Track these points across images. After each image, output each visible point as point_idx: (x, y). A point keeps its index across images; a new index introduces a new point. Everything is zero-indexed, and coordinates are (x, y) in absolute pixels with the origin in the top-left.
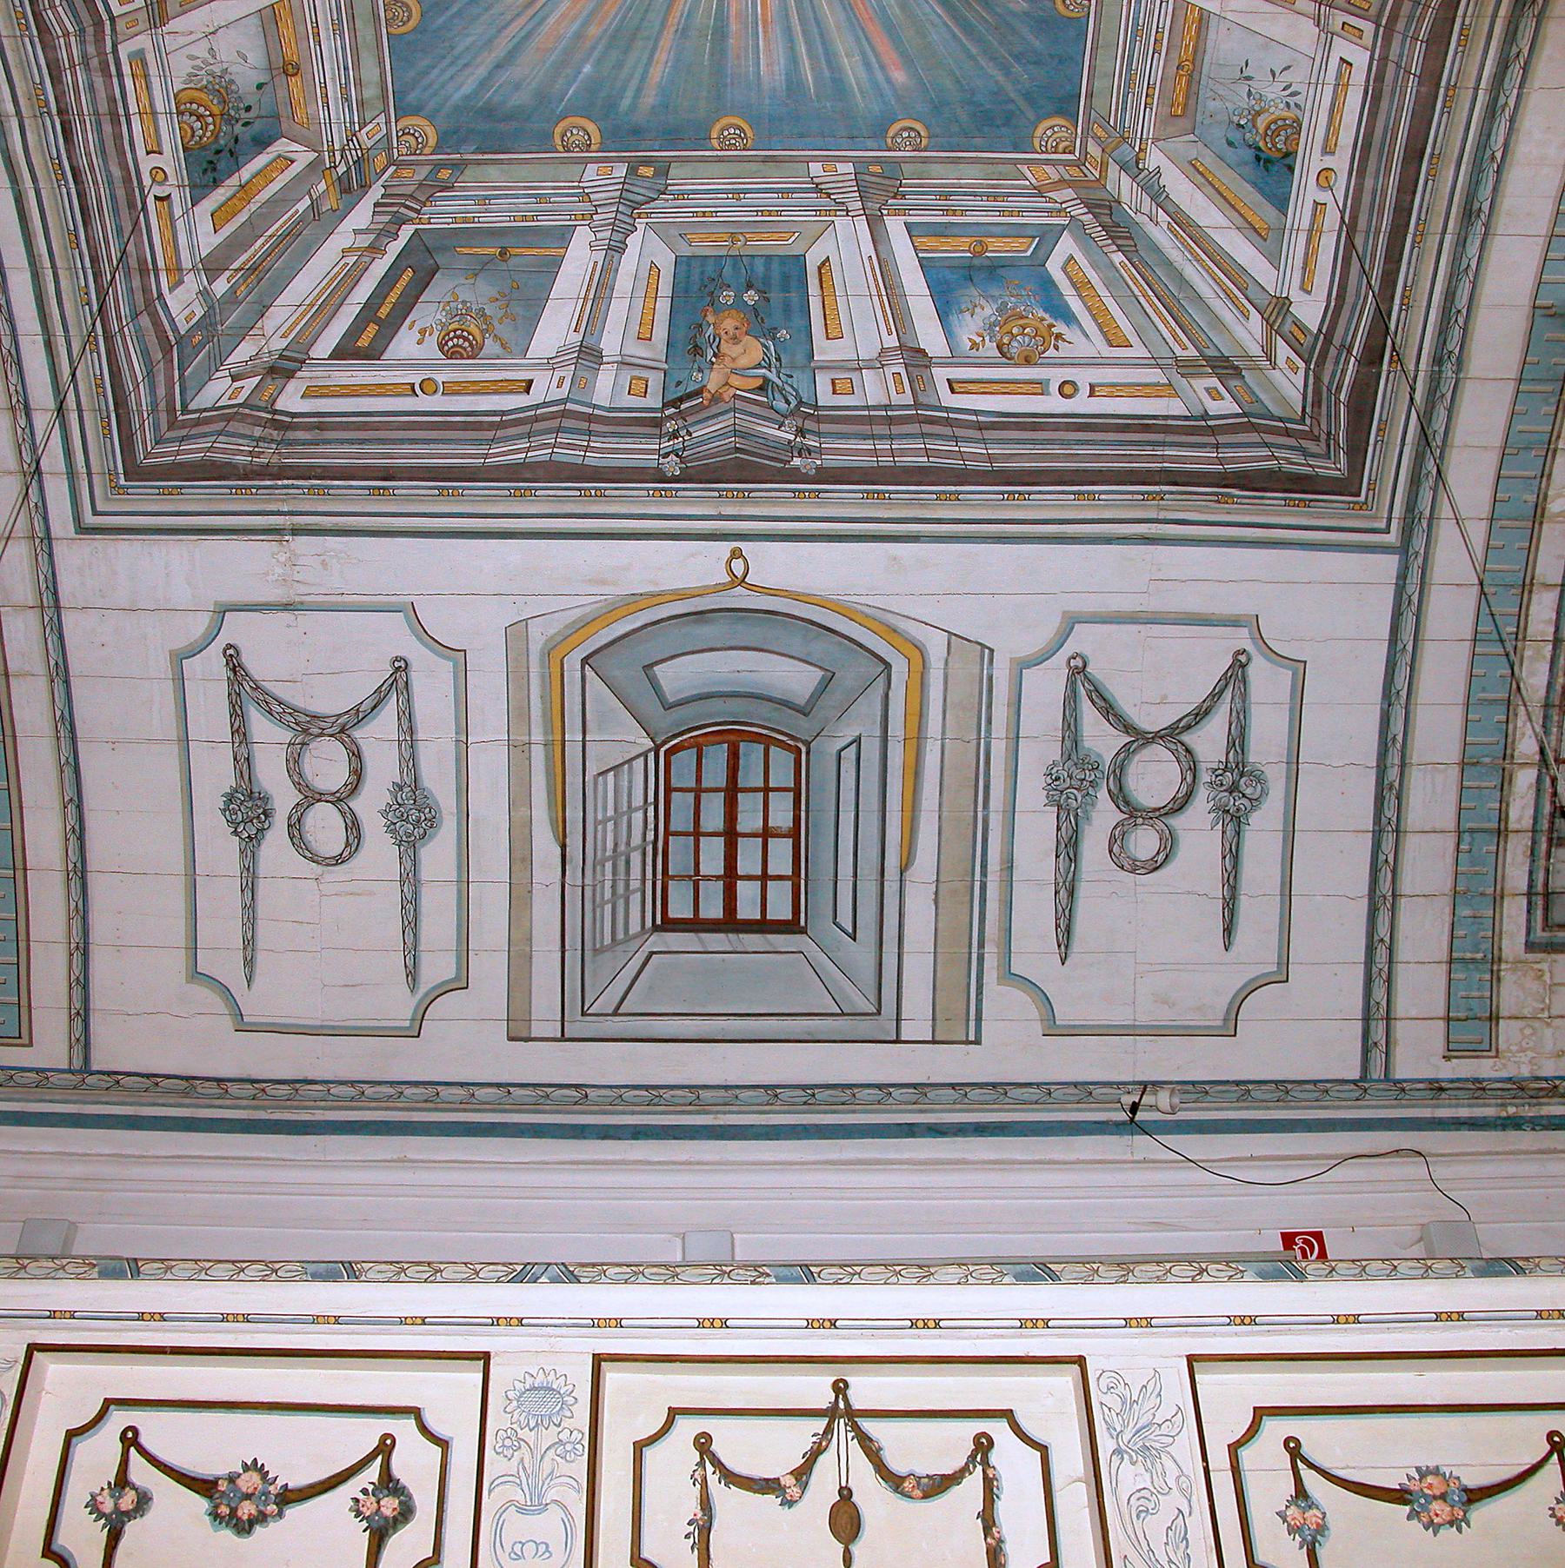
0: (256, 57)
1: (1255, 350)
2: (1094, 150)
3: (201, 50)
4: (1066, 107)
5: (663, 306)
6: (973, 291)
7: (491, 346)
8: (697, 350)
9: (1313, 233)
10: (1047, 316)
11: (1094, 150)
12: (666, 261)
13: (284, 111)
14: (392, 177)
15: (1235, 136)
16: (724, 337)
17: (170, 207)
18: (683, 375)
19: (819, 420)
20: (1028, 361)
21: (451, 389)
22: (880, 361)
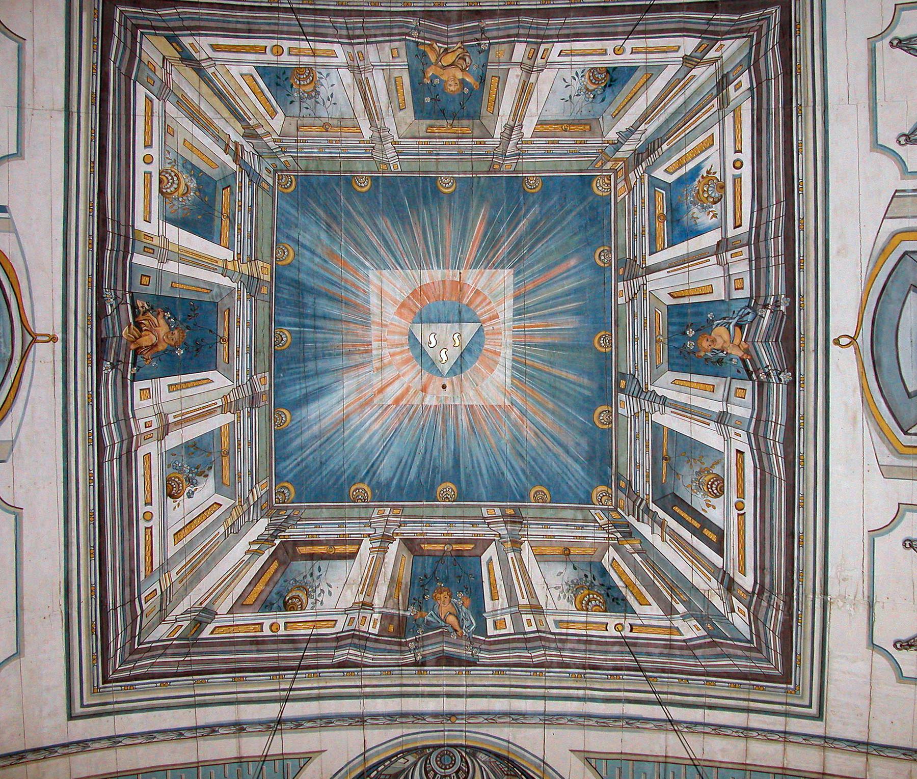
0: (560, 567)
1: (712, 69)
2: (609, 165)
3: (556, 593)
4: (586, 182)
5: (696, 378)
6: (685, 219)
7: (717, 470)
8: (720, 361)
9: (647, 51)
10: (697, 180)
11: (609, 165)
12: (670, 376)
13: (588, 559)
14: (623, 511)
15: (599, 98)
16: (712, 346)
17: (636, 625)
18: (734, 369)
19: (758, 296)
20: (723, 187)
21: (741, 493)
22: (726, 266)
